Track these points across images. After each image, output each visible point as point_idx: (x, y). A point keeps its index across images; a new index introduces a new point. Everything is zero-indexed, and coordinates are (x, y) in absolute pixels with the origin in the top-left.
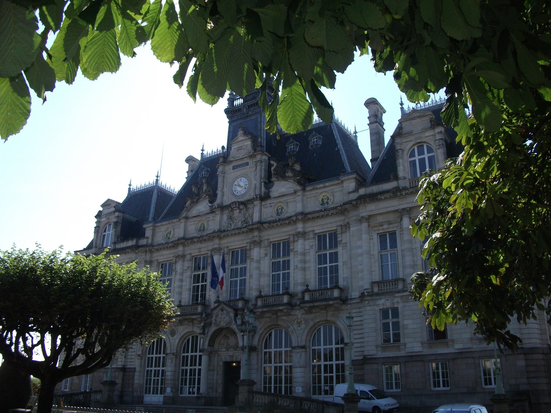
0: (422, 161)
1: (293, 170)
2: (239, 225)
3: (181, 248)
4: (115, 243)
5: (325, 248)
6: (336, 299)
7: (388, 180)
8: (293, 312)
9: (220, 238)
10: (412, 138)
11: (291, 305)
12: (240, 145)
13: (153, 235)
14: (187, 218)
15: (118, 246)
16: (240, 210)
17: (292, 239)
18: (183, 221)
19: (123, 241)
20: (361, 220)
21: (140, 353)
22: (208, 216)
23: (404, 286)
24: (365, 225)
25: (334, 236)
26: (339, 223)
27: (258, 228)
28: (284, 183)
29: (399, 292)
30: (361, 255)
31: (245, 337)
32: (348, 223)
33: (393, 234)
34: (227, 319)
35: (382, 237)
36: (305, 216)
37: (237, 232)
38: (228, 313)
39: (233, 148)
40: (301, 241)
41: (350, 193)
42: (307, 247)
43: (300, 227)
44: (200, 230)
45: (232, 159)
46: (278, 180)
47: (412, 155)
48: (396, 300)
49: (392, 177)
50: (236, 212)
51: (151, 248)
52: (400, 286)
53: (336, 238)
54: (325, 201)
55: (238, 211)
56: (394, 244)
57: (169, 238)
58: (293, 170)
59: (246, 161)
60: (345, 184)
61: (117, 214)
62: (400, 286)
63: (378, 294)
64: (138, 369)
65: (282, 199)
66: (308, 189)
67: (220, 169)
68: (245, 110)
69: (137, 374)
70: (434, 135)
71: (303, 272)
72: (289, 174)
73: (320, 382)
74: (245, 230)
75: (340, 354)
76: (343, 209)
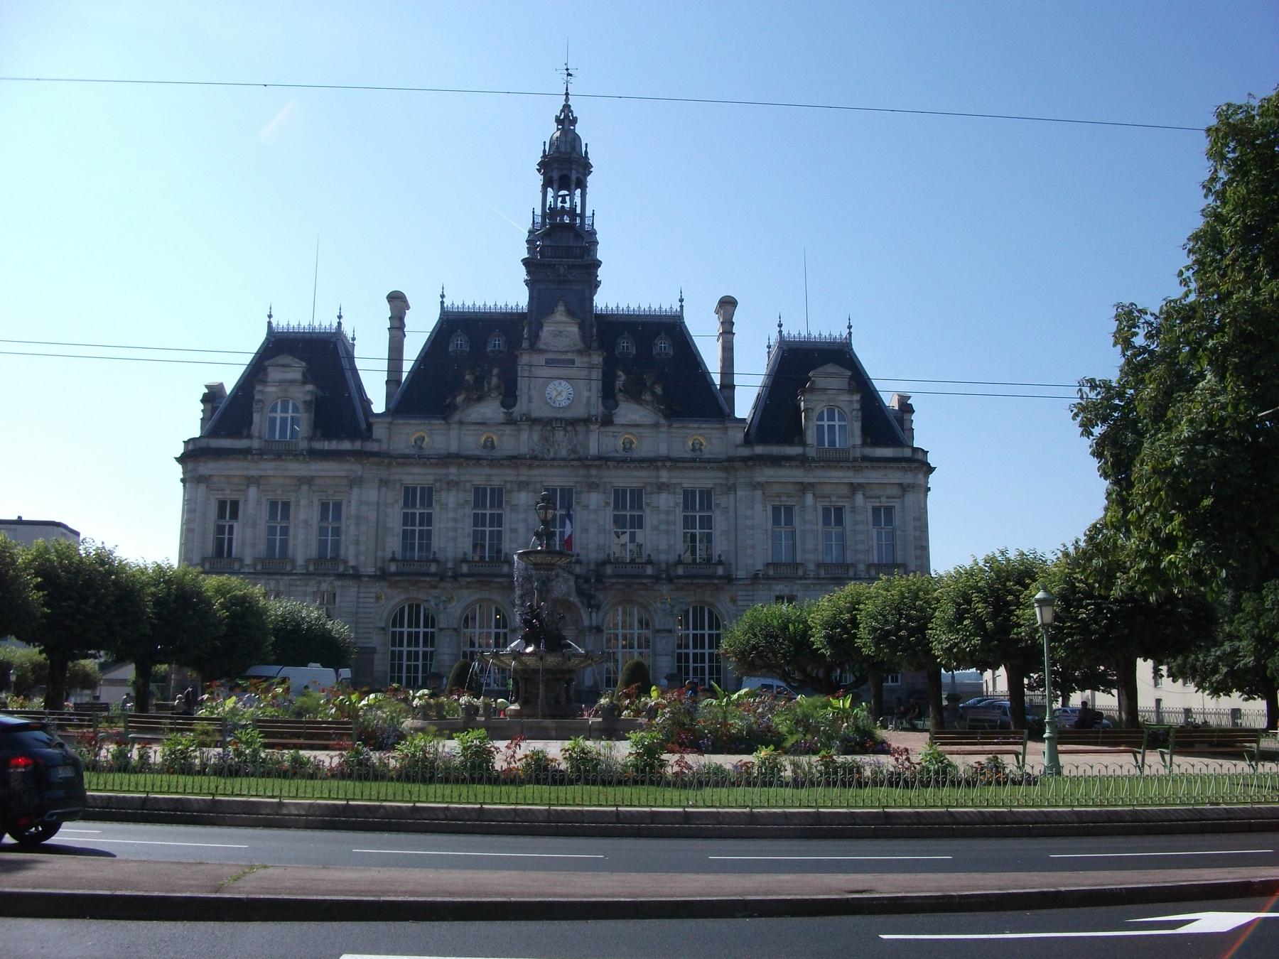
0: (831, 428)
1: (654, 394)
2: (564, 453)
3: (453, 470)
4: (310, 439)
5: (694, 508)
6: (720, 577)
7: (791, 442)
8: (656, 587)
9: (530, 467)
10: (825, 398)
11: (657, 578)
12: (561, 327)
13: (389, 438)
14: (461, 423)
15: (318, 445)
16: (566, 431)
17: (649, 489)
18: (456, 426)
19: (328, 436)
20: (754, 486)
21: (383, 625)
22: (502, 428)
23: (805, 573)
24: (758, 493)
25: (707, 495)
26: (716, 481)
27: (599, 467)
28: (635, 407)
29: (800, 579)
30: (752, 528)
31: (594, 615)
32: (734, 485)
33: (789, 510)
34: (564, 588)
35: (776, 510)
36: (673, 462)
37: (562, 463)
38: (566, 581)
39: (545, 329)
40: (664, 496)
41: (737, 446)
42: (672, 504)
43: (664, 476)
44: (485, 446)
45: (542, 346)
46: (627, 400)
47: (820, 418)
48: (795, 587)
49: (796, 439)
50: (560, 435)
51: (385, 458)
52: (800, 572)
53: (709, 498)
54: (697, 446)
55: (562, 433)
56: (789, 521)
57: (421, 448)
58: (654, 394)
59: (569, 356)
60: (731, 433)
61: (309, 387)
62: (800, 572)
63: (775, 579)
64: (380, 649)
65: (634, 430)
66: (676, 425)
67: (524, 359)
68: (562, 270)
69: (376, 656)
70: (851, 402)
71: (662, 533)
72: (647, 397)
73: (687, 673)
74: (575, 463)
75: (715, 641)
76: (727, 463)
